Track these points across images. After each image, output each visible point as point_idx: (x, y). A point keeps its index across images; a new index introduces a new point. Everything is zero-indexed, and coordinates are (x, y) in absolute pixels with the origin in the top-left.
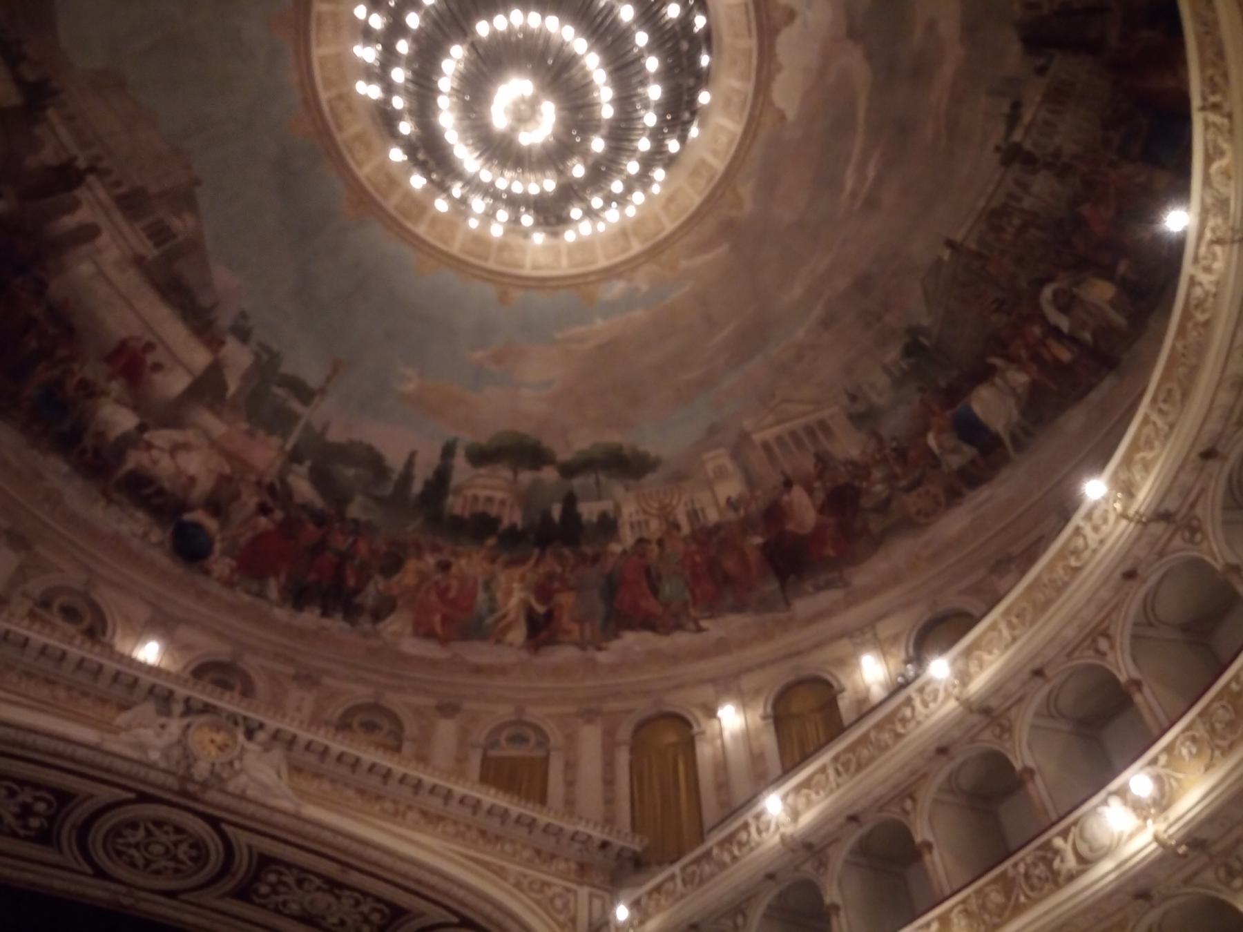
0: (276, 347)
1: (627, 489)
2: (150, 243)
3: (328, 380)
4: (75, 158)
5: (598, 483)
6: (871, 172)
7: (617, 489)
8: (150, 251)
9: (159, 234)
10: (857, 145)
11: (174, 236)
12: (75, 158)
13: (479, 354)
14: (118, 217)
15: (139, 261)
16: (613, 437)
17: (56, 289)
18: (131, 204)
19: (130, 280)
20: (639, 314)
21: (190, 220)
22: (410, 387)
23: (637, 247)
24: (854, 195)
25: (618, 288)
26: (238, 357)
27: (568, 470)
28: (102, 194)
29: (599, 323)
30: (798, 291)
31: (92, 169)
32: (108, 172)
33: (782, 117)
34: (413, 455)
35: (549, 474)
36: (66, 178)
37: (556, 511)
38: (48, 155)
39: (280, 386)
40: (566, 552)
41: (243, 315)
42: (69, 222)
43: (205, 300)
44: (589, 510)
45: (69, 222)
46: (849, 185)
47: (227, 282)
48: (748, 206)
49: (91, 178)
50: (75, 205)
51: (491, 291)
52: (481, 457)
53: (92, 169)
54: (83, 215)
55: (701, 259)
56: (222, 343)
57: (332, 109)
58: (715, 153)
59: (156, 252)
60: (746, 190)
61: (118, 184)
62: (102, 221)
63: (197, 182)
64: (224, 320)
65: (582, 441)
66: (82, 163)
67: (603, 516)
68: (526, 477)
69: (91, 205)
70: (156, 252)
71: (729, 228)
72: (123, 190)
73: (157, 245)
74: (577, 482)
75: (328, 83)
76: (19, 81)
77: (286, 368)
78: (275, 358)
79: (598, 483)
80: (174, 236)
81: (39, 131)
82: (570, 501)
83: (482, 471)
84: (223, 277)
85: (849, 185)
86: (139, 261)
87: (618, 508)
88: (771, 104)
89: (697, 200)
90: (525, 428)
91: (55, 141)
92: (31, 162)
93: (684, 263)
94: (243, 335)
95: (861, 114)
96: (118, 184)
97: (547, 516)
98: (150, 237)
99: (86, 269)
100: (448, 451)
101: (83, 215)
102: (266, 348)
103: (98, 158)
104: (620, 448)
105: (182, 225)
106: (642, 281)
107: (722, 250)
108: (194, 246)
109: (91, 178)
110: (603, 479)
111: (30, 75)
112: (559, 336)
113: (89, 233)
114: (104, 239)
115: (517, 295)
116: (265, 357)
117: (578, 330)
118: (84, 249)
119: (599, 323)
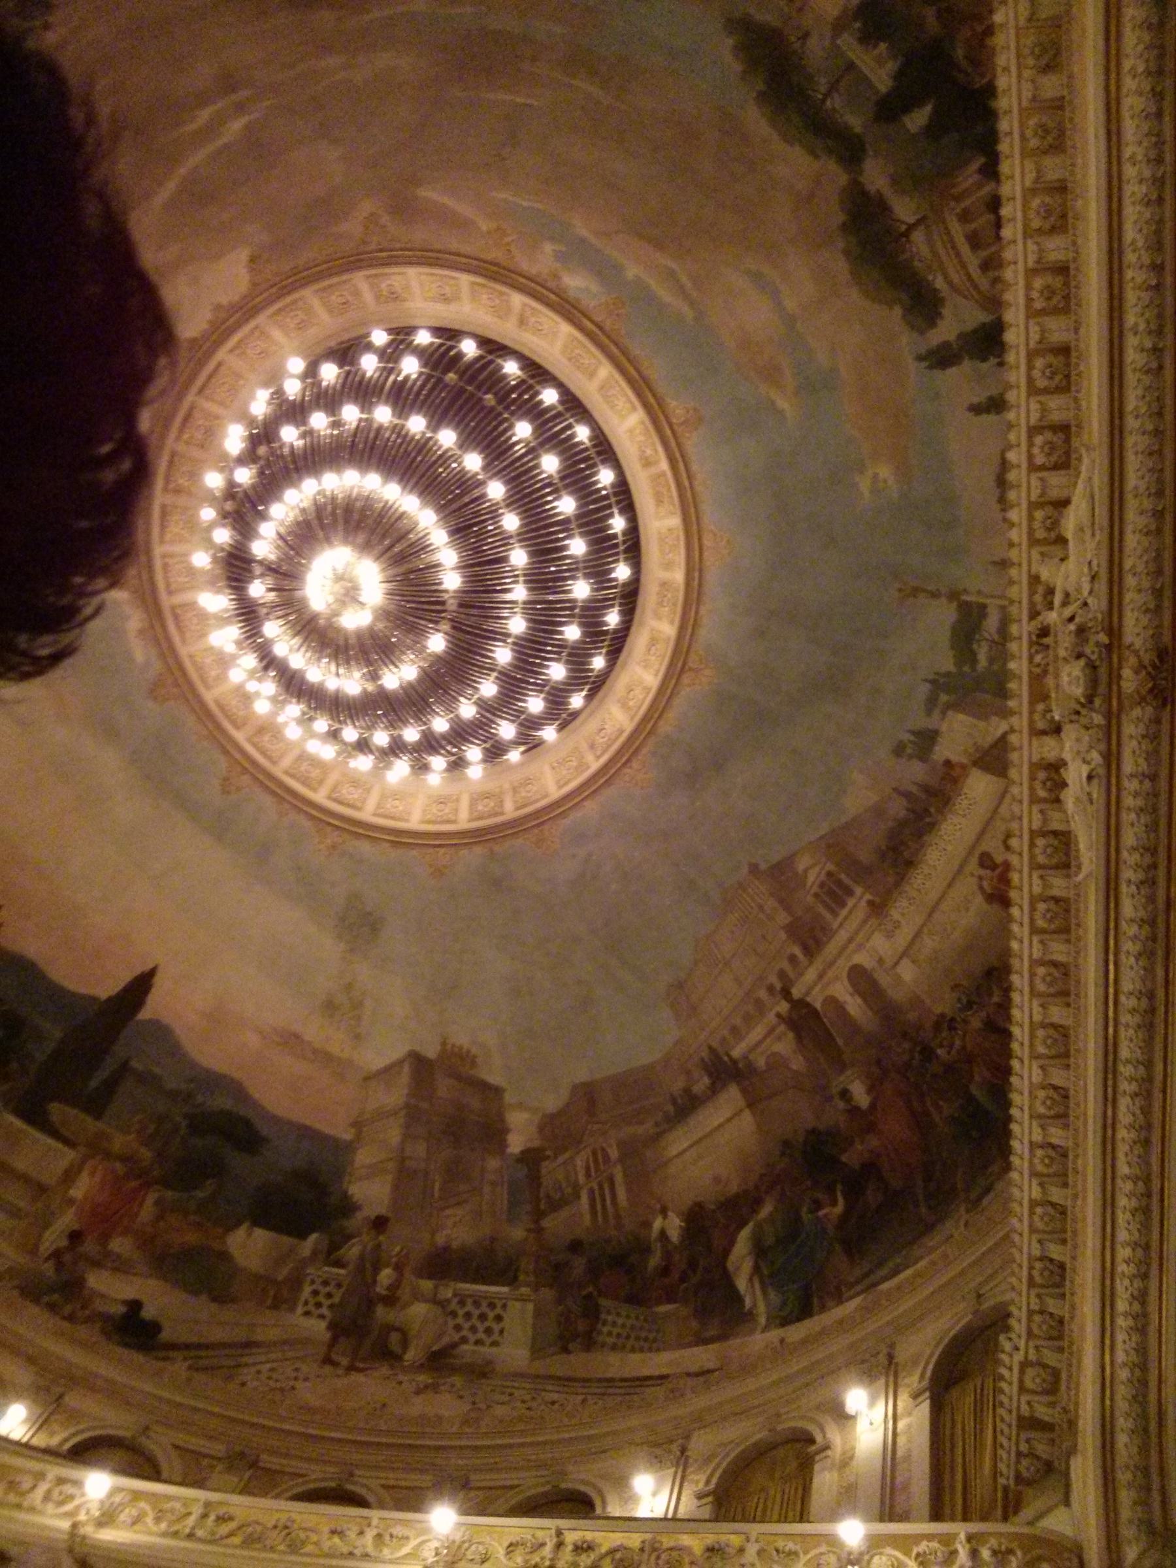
0: (925, 688)
1: (806, 35)
2: (851, 902)
3: (935, 595)
4: (778, 1015)
5: (833, 88)
6: (204, 115)
7: (816, 49)
8: (860, 899)
9: (835, 894)
10: (197, 158)
11: (829, 874)
12: (778, 1015)
13: (783, 404)
14: (832, 948)
15: (878, 908)
16: (756, 121)
17: (945, 1004)
18: (810, 938)
19: (906, 912)
20: (581, 228)
21: (802, 864)
22: (885, 471)
23: (517, 300)
24: (240, 108)
25: (576, 282)
26: (959, 734)
27: (850, 151)
28: (811, 975)
29: (632, 271)
30: (384, 59)
31: (786, 993)
32: (782, 975)
33: (253, 259)
34: (976, 409)
35: (875, 176)
36: (805, 1021)
37: (918, 119)
38: (785, 1046)
39: (974, 661)
40: (960, 53)
41: (899, 750)
42: (854, 1006)
43: (898, 808)
44: (879, 70)
45: (854, 1006)
46: (236, 126)
47: (865, 790)
48: (367, 207)
49: (796, 993)
50: (831, 1001)
51: (693, 442)
52: (923, 304)
53: (786, 993)
54: (842, 991)
55: (464, 209)
56: (948, 763)
57: (604, 752)
58: (357, 293)
59: (858, 890)
60: (352, 227)
61: (793, 959)
62: (843, 966)
63: (754, 869)
64: (915, 772)
65: (796, 165)
66: (784, 1007)
67: (867, 39)
68: (904, 210)
69: (827, 985)
70: (858, 890)
71: (404, 208)
72: (797, 951)
73: (850, 892)
74: (855, 122)
75: (582, 767)
76: (714, 1090)
77: (948, 664)
78: (939, 684)
79: (833, 88)
80: (829, 874)
81: (761, 1063)
82: (889, 109)
83: (939, 283)
84: (859, 797)
85: (236, 126)
86: (878, 908)
87: (839, 26)
88: (255, 285)
89: (412, 272)
90: (841, 266)
91: (766, 1041)
92: (798, 1063)
93: (484, 226)
94: (927, 739)
95: (171, 186)
96: (793, 959)
97: (934, 130)
98: (843, 904)
99: (907, 972)
100: (942, 358)
101: (842, 991)
102: (931, 703)
103: (771, 989)
104: (762, 98)
105: (813, 870)
106: (542, 260)
107: (428, 193)
108: (834, 844)
109: (796, 993)
110: (823, 84)
111: (703, 1083)
112: (689, 313)
113: (861, 979)
114: (862, 959)
115: (677, 408)
116: (944, 698)
117: (665, 295)
118: (884, 980)
119: (632, 271)
